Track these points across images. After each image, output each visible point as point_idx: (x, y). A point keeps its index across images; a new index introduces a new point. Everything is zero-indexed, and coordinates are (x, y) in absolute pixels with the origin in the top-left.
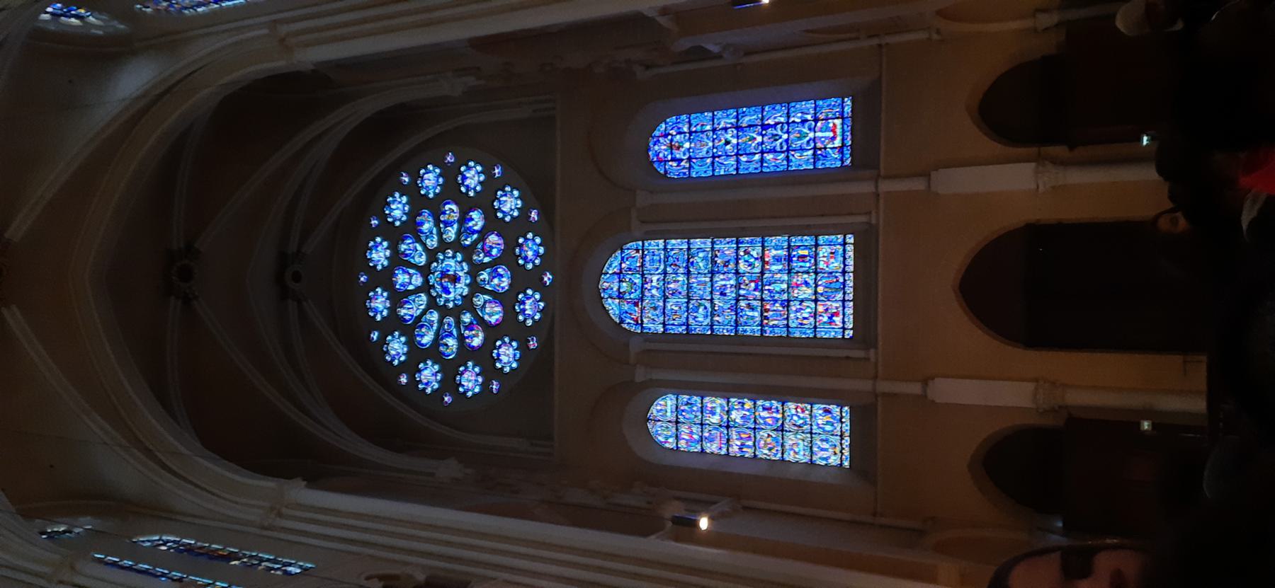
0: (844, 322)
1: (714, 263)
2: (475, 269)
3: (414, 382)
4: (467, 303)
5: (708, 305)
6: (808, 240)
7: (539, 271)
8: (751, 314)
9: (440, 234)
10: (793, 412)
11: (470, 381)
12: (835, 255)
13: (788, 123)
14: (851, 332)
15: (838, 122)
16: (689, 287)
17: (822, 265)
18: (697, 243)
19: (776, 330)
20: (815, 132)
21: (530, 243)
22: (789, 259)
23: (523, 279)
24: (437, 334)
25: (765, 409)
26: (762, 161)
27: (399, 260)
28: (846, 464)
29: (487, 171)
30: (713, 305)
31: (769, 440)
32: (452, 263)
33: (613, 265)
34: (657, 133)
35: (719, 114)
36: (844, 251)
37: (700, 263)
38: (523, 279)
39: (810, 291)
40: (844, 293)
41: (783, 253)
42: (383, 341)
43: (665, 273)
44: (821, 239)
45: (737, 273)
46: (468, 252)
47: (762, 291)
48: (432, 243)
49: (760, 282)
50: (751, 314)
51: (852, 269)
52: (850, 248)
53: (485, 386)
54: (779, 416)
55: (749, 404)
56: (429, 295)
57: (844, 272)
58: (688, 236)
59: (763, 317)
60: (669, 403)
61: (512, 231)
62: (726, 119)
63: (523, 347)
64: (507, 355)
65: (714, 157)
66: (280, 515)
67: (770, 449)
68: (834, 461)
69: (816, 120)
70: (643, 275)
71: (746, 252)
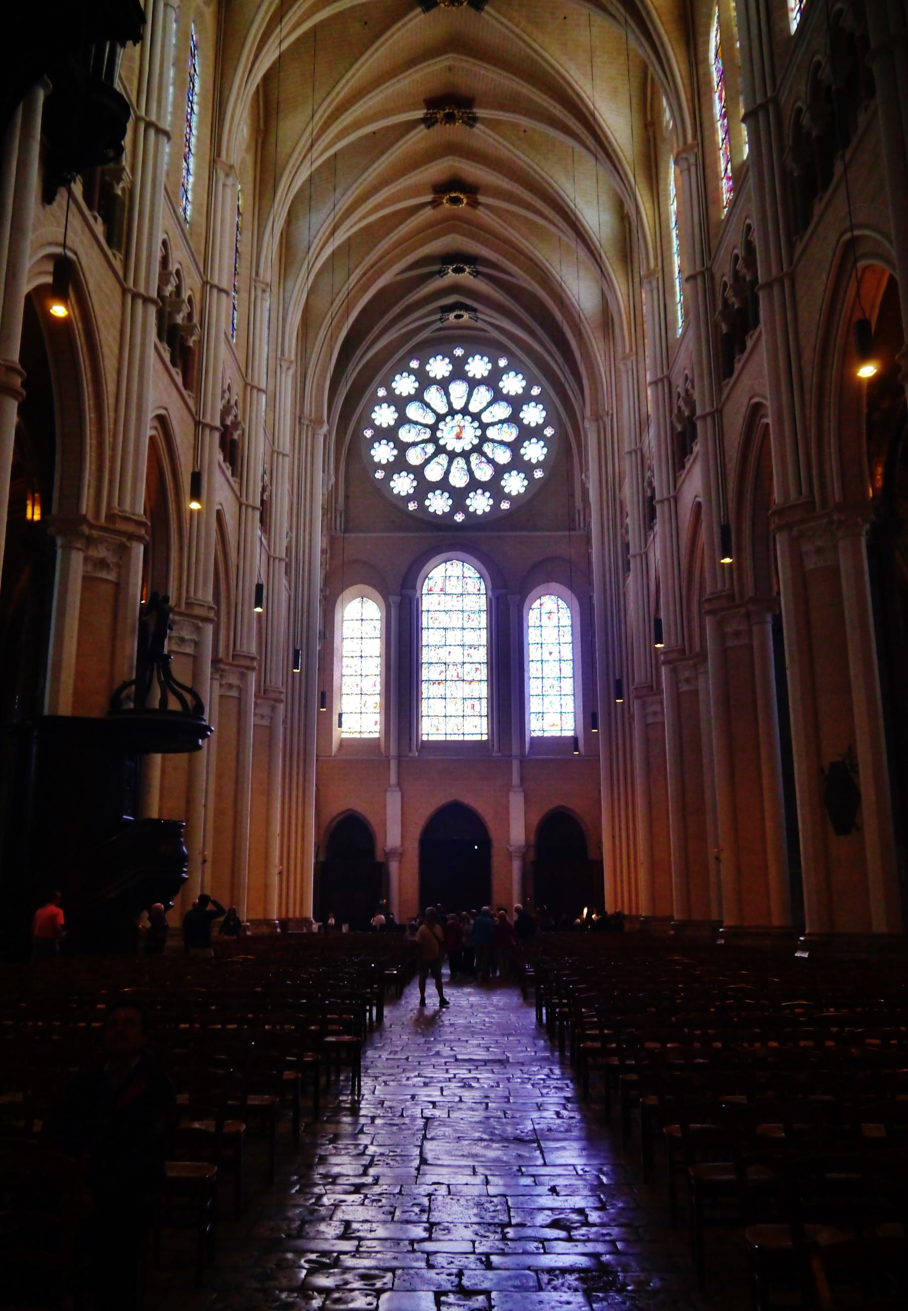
1: (471, 647)
2: (466, 455)
3: (380, 401)
4: (440, 450)
6: (484, 712)
7: (465, 509)
9: (493, 424)
11: (383, 453)
12: (475, 727)
18: (484, 634)
21: (486, 502)
23: (459, 496)
24: (416, 423)
27: (473, 384)
28: (344, 736)
29: (539, 465)
30: (440, 647)
32: (471, 436)
33: (470, 572)
34: (560, 602)
35: (569, 647)
37: (471, 638)
38: (459, 496)
42: (411, 372)
45: (464, 663)
46: (477, 449)
48: (486, 418)
52: (478, 738)
53: (379, 466)
55: (378, 671)
56: (446, 415)
61: (493, 487)
62: (567, 652)
63: (409, 498)
64: (403, 484)
66: (307, 426)
70: (462, 594)
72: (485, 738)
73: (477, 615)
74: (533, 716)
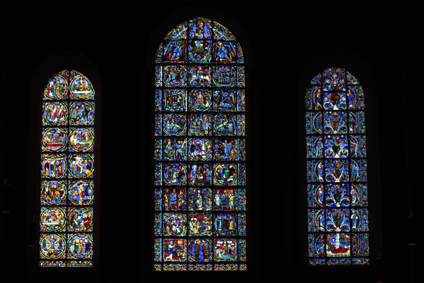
0: (168, 263)
1: (223, 139)
5: (181, 134)
8: (174, 176)
10: (85, 216)
13: (350, 207)
14: (159, 269)
15: (348, 253)
16: (199, 114)
17: (220, 242)
19: (160, 201)
20: (338, 232)
22: (225, 211)
25: (86, 188)
26: (318, 183)
30: (182, 138)
31: (57, 193)
34: (349, 76)
36: (232, 263)
39: (196, 231)
40: (194, 263)
41: (232, 203)
43: (213, 88)
44: (243, 242)
47: (195, 187)
49: (206, 185)
50: (174, 176)
51: (216, 269)
52: (235, 267)
54: (80, 203)
57: (213, 263)
58: (249, 113)
59: (172, 188)
60: (86, 92)
62: (358, 148)
65: (323, 135)
67: (48, 194)
68: (44, 253)
69: (351, 233)
71: (232, 171)
72: (243, 268)
73: (232, 95)
74: (311, 237)
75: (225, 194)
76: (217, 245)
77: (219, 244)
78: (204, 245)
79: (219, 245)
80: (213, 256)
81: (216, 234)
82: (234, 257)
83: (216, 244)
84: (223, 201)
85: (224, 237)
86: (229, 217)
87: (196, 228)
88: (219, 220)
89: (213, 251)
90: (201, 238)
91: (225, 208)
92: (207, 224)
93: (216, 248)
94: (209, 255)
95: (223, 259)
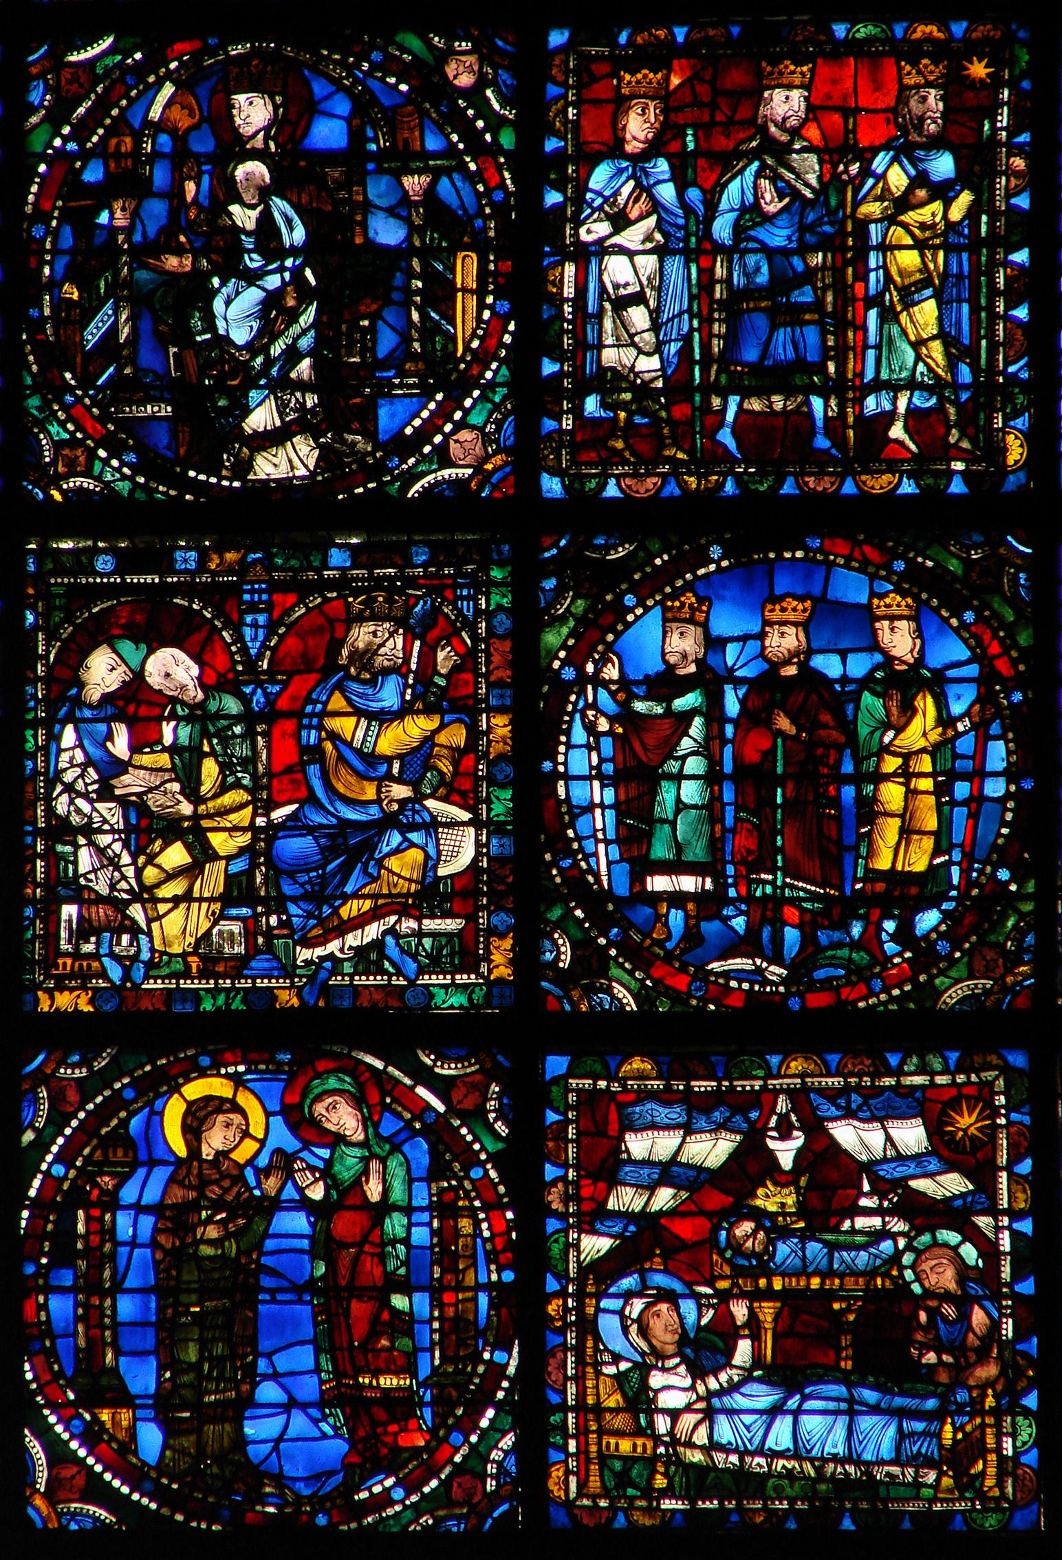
75: (774, 153)
76: (625, 1199)
77: (668, 1172)
78: (346, 1195)
79: (664, 1198)
80: (532, 1414)
81: (591, 966)
82: (971, 1448)
83: (608, 1166)
84: (737, 303)
85: (760, 1027)
86: (865, 617)
87: (176, 855)
88: (666, 683)
89: (522, 1313)
90: (293, 1040)
91: (776, 442)
92: (417, 760)
93: (595, 1245)
94: (458, 1395)
95: (743, 1482)
